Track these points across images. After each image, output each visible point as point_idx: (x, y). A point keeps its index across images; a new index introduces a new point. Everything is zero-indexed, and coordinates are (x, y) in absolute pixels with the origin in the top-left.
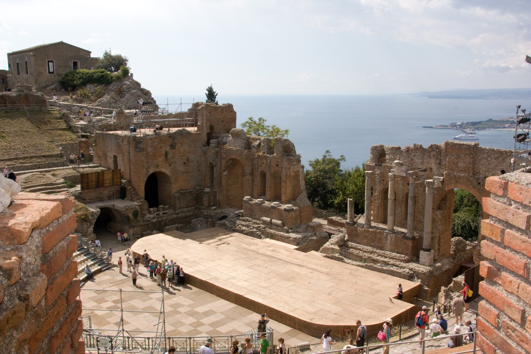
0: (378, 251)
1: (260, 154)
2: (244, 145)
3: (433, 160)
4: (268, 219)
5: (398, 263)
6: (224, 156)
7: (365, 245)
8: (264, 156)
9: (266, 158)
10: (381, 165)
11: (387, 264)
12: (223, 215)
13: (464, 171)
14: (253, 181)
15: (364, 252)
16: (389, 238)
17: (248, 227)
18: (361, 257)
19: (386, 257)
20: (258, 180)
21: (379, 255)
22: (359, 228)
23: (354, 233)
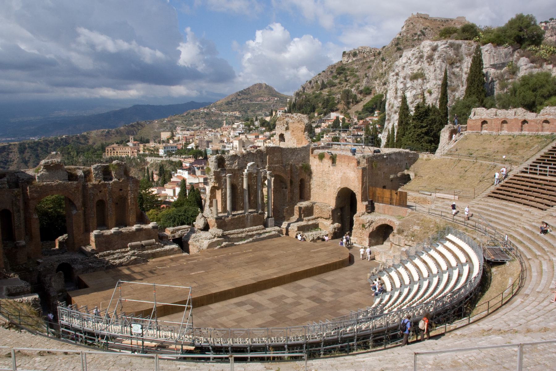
0: (244, 230)
1: (94, 182)
2: (67, 178)
3: (259, 159)
4: (138, 243)
5: (265, 231)
6: (35, 195)
7: (232, 230)
8: (102, 184)
9: (105, 185)
10: (225, 170)
11: (261, 234)
12: (58, 264)
13: (277, 163)
14: (85, 214)
15: (237, 234)
16: (249, 218)
17: (120, 258)
18: (238, 238)
19: (253, 231)
20: (93, 212)
21: (248, 232)
22: (226, 219)
23: (221, 223)
